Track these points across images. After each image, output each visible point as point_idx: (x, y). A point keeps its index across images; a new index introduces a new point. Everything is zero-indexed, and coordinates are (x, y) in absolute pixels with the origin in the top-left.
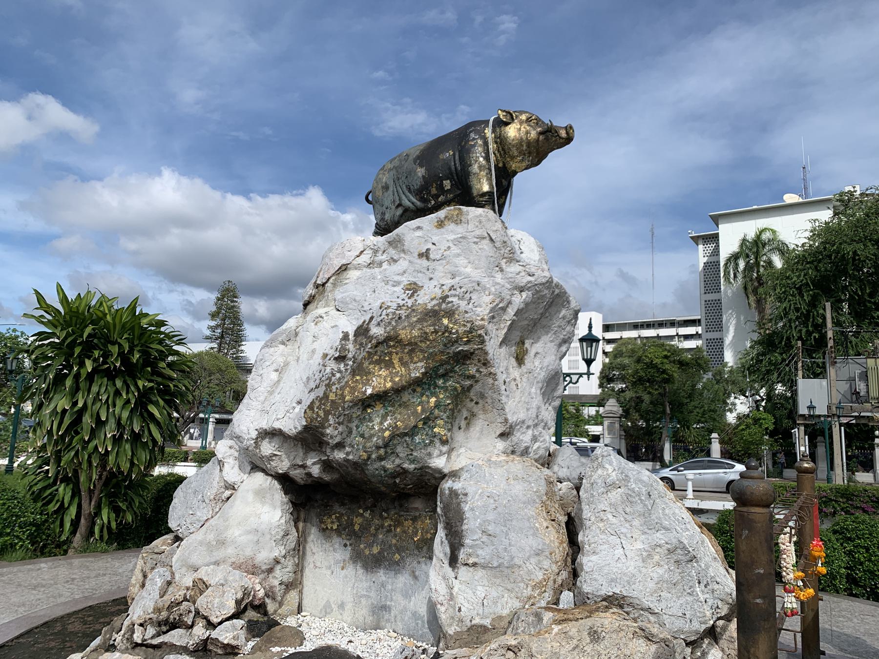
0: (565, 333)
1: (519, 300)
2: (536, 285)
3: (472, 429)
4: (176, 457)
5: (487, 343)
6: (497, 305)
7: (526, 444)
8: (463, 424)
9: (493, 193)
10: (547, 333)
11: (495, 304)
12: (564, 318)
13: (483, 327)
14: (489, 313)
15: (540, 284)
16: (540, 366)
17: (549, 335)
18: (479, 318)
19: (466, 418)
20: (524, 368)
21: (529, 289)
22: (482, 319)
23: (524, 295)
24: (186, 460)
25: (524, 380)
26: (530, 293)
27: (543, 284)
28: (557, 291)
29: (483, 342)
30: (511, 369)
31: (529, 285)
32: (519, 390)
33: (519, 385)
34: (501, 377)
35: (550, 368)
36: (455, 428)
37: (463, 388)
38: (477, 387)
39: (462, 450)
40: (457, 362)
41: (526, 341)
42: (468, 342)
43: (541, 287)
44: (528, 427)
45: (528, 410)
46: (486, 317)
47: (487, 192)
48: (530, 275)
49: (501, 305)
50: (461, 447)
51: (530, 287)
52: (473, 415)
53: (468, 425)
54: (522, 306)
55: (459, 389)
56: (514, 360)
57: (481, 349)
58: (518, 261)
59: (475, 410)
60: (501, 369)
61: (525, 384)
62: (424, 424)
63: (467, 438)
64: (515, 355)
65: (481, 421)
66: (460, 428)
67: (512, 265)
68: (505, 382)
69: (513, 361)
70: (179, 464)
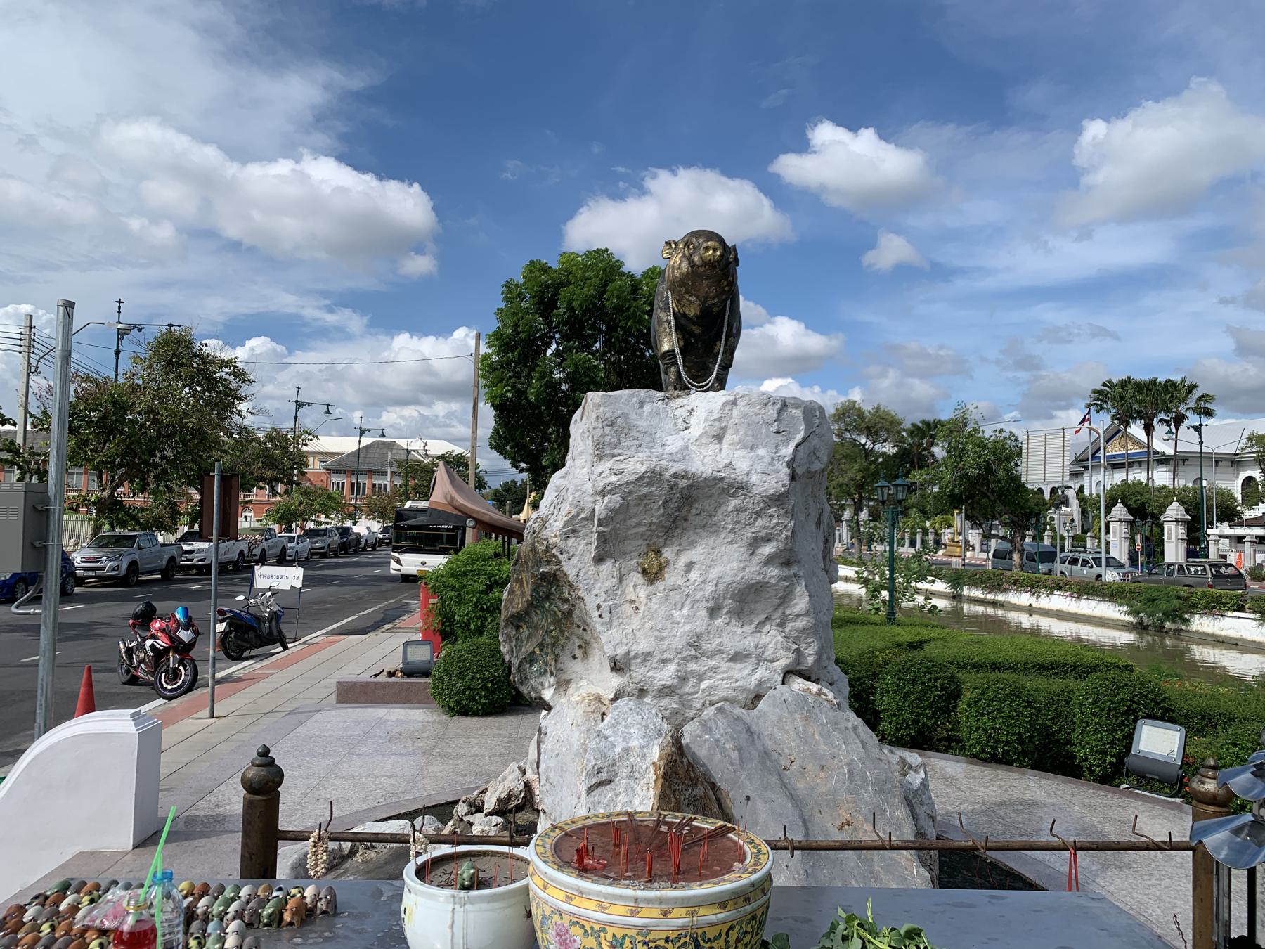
0: (754, 530)
1: (601, 507)
2: (622, 485)
3: (591, 659)
4: (1224, 604)
5: (563, 563)
6: (578, 516)
7: (663, 682)
8: (578, 652)
9: (674, 351)
10: (717, 533)
11: (570, 516)
12: (739, 510)
13: (555, 545)
14: (564, 527)
15: (627, 484)
16: (701, 579)
17: (723, 535)
18: (553, 535)
19: (580, 647)
20: (660, 585)
21: (610, 492)
22: (556, 536)
23: (606, 499)
24: (1241, 609)
25: (654, 600)
26: (614, 497)
27: (632, 483)
28: (684, 483)
29: (559, 562)
30: (631, 589)
31: (609, 488)
32: (640, 615)
33: (642, 609)
34: (591, 603)
35: (727, 580)
36: (565, 659)
37: (563, 613)
38: (577, 611)
39: (584, 683)
40: (552, 583)
41: (664, 550)
42: (548, 562)
43: (630, 487)
44: (664, 661)
45: (661, 639)
46: (558, 534)
47: (668, 351)
48: (615, 474)
49: (582, 516)
50: (581, 679)
51: (611, 490)
52: (588, 644)
53: (585, 654)
54: (604, 515)
55: (560, 614)
56: (640, 575)
57: (559, 569)
58: (613, 456)
59: (587, 636)
60: (595, 591)
61: (656, 606)
62: (541, 650)
63: (587, 670)
64: (640, 570)
65: (597, 650)
66: (574, 657)
67: (602, 463)
68: (599, 607)
69: (638, 578)
70: (1230, 614)
